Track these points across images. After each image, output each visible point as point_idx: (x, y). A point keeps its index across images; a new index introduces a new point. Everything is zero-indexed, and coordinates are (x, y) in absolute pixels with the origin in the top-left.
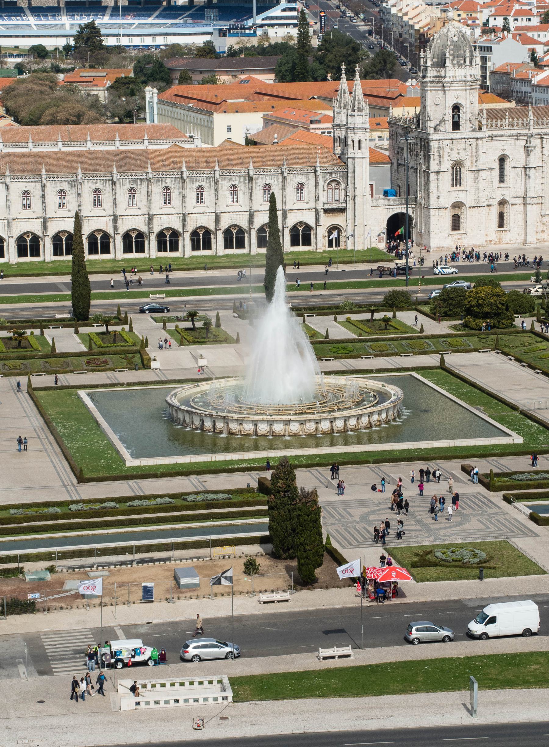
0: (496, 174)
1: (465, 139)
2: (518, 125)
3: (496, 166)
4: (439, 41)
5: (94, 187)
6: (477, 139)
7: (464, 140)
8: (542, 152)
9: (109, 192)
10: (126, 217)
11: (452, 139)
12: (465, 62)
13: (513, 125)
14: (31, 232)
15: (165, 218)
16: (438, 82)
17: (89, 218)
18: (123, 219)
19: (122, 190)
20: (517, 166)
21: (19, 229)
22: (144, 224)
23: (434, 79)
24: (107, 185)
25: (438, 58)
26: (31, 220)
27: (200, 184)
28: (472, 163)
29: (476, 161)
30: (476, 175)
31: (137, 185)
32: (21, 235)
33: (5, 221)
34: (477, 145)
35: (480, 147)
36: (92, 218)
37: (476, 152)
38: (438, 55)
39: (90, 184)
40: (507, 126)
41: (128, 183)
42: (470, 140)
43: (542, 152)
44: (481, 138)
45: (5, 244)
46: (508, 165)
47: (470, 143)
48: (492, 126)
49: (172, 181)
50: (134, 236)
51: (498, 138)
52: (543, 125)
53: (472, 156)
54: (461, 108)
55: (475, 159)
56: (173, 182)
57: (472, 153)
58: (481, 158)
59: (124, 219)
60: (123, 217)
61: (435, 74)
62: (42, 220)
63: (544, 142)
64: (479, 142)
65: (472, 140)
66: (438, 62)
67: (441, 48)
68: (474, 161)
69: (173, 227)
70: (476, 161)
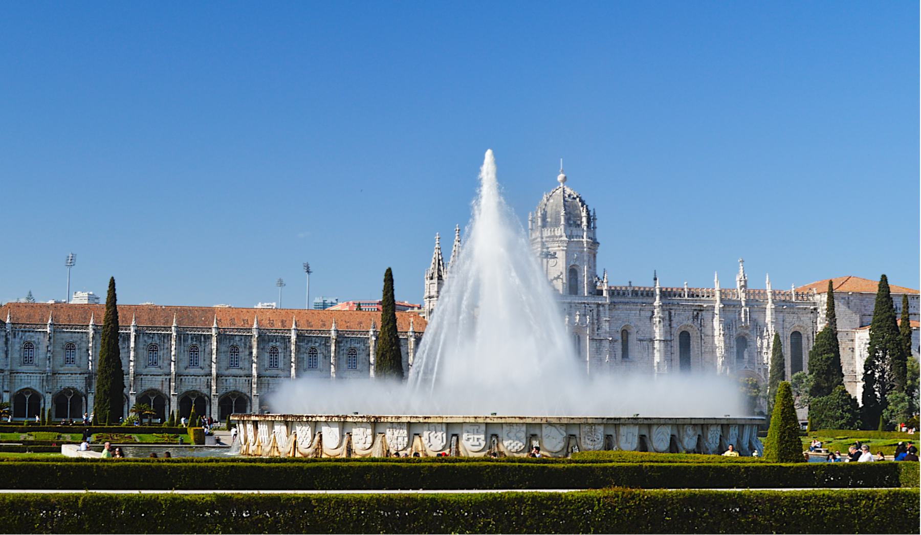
0: (619, 346)
1: (584, 303)
2: (642, 294)
3: (619, 337)
4: (551, 201)
5: (150, 341)
6: (598, 305)
7: (583, 305)
8: (670, 325)
9: (167, 348)
10: (186, 377)
11: (570, 303)
12: (581, 222)
13: (637, 294)
14: (73, 389)
15: (231, 381)
16: (553, 241)
17: (142, 376)
18: (181, 379)
19: (182, 347)
20: (642, 338)
21: (59, 385)
22: (206, 387)
23: (548, 239)
24: (166, 341)
25: (551, 218)
26: (74, 375)
27: (274, 344)
28: (593, 330)
29: (598, 329)
30: (598, 345)
31: (201, 342)
32: (61, 391)
33: (43, 375)
34: (598, 311)
35: (602, 314)
36: (145, 377)
37: (597, 320)
38: (551, 215)
39: (146, 338)
40: (630, 295)
41: (190, 339)
42: (590, 305)
43: (670, 325)
44: (603, 305)
45: (42, 401)
46: (633, 339)
47: (591, 309)
48: (613, 294)
49: (241, 339)
50: (193, 399)
51: (621, 306)
52: (670, 296)
53: (593, 324)
54: (578, 270)
55: (596, 327)
56: (243, 341)
57: (593, 320)
58: (604, 327)
59: (183, 380)
60: (182, 377)
61: (549, 234)
62: (86, 375)
63: (673, 314)
64: (601, 308)
65: (592, 305)
66: (551, 222)
67: (554, 207)
68: (596, 329)
69: (240, 390)
70: (598, 329)
